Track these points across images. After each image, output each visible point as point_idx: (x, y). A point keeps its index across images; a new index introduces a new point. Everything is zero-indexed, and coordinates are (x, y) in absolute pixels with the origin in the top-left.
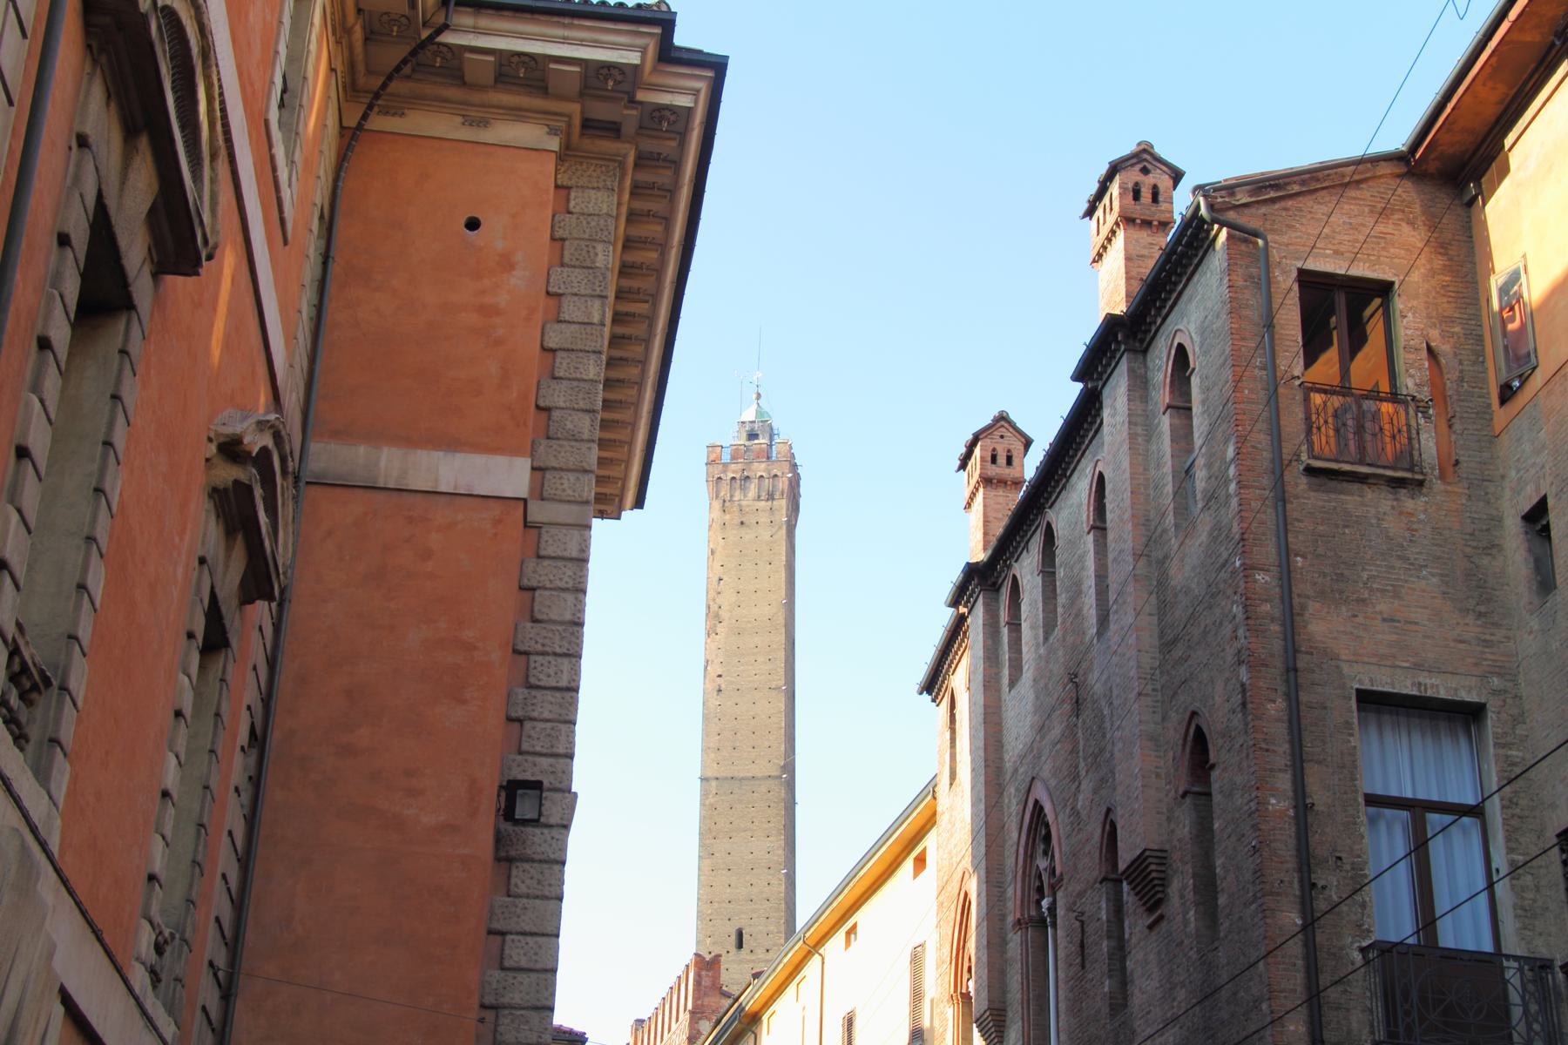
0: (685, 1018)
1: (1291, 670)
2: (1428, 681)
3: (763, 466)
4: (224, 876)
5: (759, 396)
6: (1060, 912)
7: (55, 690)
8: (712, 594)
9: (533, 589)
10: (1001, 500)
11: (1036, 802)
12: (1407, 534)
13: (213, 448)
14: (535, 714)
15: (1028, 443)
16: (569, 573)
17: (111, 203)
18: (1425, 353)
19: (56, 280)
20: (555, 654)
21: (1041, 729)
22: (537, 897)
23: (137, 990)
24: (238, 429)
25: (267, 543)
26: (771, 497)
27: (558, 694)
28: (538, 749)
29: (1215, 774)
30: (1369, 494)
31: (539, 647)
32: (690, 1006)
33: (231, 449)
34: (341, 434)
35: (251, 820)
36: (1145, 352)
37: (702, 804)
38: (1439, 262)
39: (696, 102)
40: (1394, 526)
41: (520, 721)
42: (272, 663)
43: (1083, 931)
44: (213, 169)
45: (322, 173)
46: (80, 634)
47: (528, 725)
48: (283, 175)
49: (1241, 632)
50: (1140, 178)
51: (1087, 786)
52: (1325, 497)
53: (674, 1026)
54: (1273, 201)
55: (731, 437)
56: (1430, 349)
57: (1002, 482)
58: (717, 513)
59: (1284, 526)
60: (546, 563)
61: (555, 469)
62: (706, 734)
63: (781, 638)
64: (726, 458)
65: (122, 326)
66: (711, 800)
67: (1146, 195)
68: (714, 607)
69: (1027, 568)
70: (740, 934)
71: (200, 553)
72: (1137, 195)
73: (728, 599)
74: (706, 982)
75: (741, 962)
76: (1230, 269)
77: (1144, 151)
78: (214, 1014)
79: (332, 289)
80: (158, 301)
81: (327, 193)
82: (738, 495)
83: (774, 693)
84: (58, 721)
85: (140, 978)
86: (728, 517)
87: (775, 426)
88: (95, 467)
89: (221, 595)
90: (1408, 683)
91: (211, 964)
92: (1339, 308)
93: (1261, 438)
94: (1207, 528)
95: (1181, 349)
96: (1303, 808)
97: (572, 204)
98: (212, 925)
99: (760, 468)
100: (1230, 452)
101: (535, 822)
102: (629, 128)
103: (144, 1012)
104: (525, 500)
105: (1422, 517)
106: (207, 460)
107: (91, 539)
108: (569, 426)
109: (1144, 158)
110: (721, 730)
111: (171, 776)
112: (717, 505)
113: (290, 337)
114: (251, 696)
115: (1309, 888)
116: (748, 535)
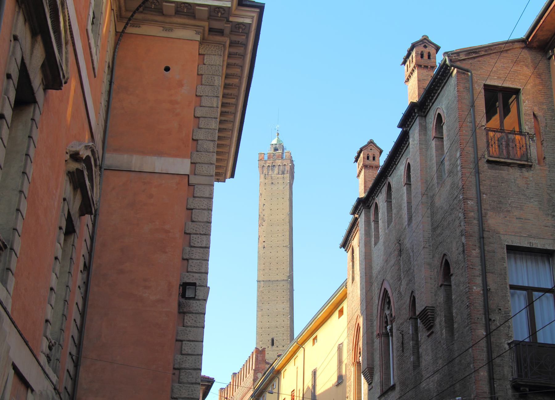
0: (252, 372)
1: (482, 238)
2: (534, 242)
3: (280, 161)
4: (75, 320)
5: (278, 134)
6: (394, 331)
7: (8, 250)
8: (261, 210)
9: (192, 209)
10: (371, 173)
11: (385, 289)
12: (526, 186)
13: (68, 156)
14: (193, 257)
15: (381, 152)
16: (205, 203)
17: (27, 62)
18: (532, 116)
19: (6, 92)
20: (200, 234)
21: (386, 261)
22: (195, 327)
23: (42, 364)
24: (78, 149)
25: (89, 193)
26: (283, 173)
27: (202, 250)
28: (194, 270)
29: (453, 278)
30: (511, 170)
31: (195, 232)
32: (254, 368)
33: (75, 157)
35: (85, 299)
36: (425, 116)
37: (258, 291)
38: (538, 81)
39: (253, 21)
41: (187, 260)
42: (92, 238)
43: (403, 338)
44: (66, 49)
45: (109, 50)
46: (18, 228)
47: (190, 261)
48: (94, 50)
49: (462, 224)
50: (423, 49)
51: (404, 282)
52: (494, 171)
53: (248, 375)
54: (474, 58)
55: (268, 150)
56: (534, 115)
57: (371, 167)
58: (263, 180)
59: (479, 183)
60: (197, 199)
61: (199, 163)
62: (259, 264)
63: (288, 227)
64: (266, 158)
65: (32, 109)
66: (261, 289)
67: (426, 56)
68: (262, 216)
69: (381, 199)
70: (273, 340)
71: (64, 196)
72: (422, 56)
74: (260, 358)
75: (273, 351)
76: (458, 84)
77: (425, 39)
78: (72, 373)
79: (113, 94)
80: (46, 100)
81: (111, 58)
82: (270, 172)
83: (285, 248)
84: (10, 261)
85: (43, 359)
86: (267, 181)
87: (284, 146)
88: (23, 164)
89: (72, 213)
90: (526, 242)
91: (70, 354)
92: (499, 99)
93: (470, 149)
94: (450, 184)
95: (439, 115)
96: (486, 290)
97: (205, 61)
98: (70, 339)
99: (279, 162)
100: (458, 154)
101: (194, 298)
102: (227, 31)
103: (45, 372)
104: (188, 175)
105: (531, 179)
106: (66, 161)
107: (21, 192)
108: (205, 146)
109: (425, 42)
110: (265, 263)
111: (54, 282)
112: (263, 176)
113: (97, 114)
114: (84, 251)
115: (489, 320)
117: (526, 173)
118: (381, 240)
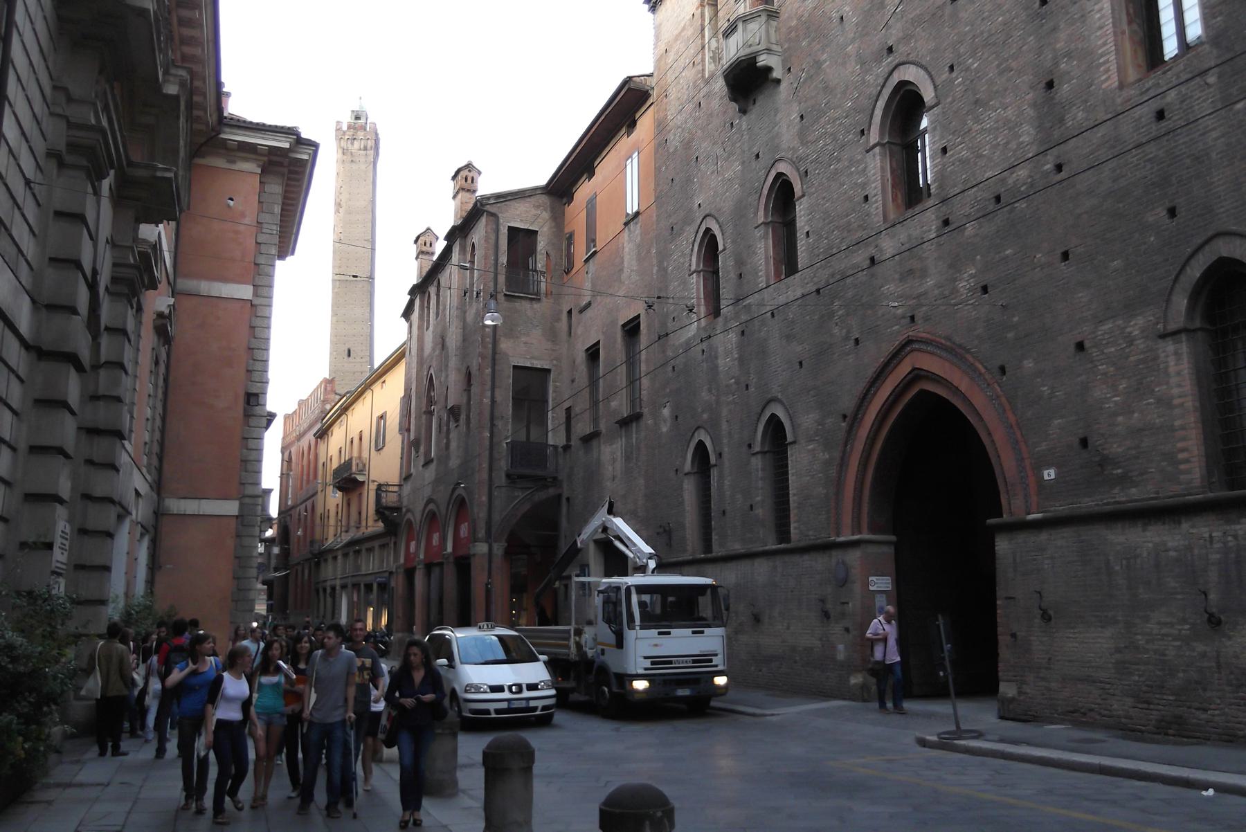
1: (494, 360)
26: (365, 149)
34: (186, 276)
40: (530, 313)
55: (347, 119)
64: (345, 128)
67: (469, 180)
69: (432, 290)
73: (344, 197)
85: (144, 470)
92: (522, 240)
93: (492, 284)
96: (493, 401)
102: (286, 163)
109: (469, 166)
112: (340, 151)
113: (168, 245)
115: (493, 425)
116: (355, 166)
117: (536, 306)
118: (431, 328)
